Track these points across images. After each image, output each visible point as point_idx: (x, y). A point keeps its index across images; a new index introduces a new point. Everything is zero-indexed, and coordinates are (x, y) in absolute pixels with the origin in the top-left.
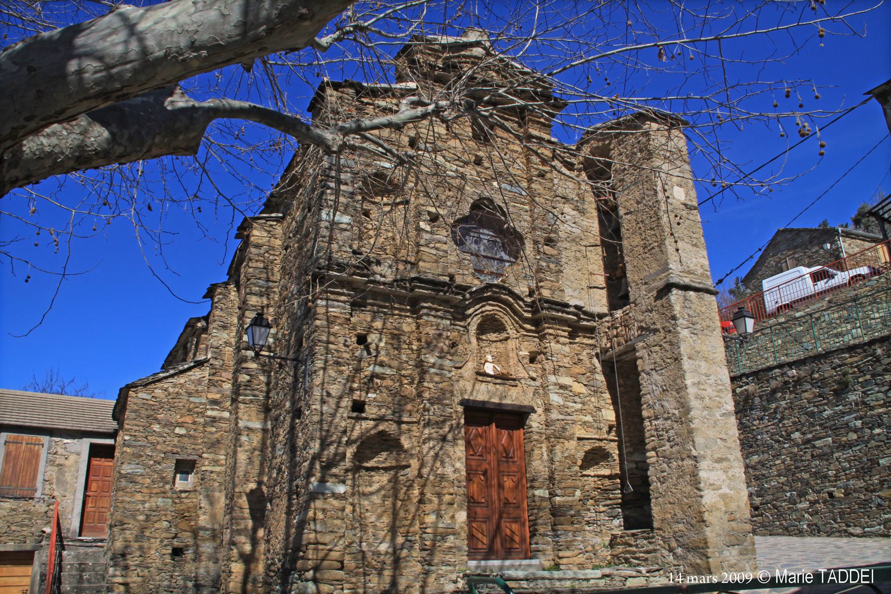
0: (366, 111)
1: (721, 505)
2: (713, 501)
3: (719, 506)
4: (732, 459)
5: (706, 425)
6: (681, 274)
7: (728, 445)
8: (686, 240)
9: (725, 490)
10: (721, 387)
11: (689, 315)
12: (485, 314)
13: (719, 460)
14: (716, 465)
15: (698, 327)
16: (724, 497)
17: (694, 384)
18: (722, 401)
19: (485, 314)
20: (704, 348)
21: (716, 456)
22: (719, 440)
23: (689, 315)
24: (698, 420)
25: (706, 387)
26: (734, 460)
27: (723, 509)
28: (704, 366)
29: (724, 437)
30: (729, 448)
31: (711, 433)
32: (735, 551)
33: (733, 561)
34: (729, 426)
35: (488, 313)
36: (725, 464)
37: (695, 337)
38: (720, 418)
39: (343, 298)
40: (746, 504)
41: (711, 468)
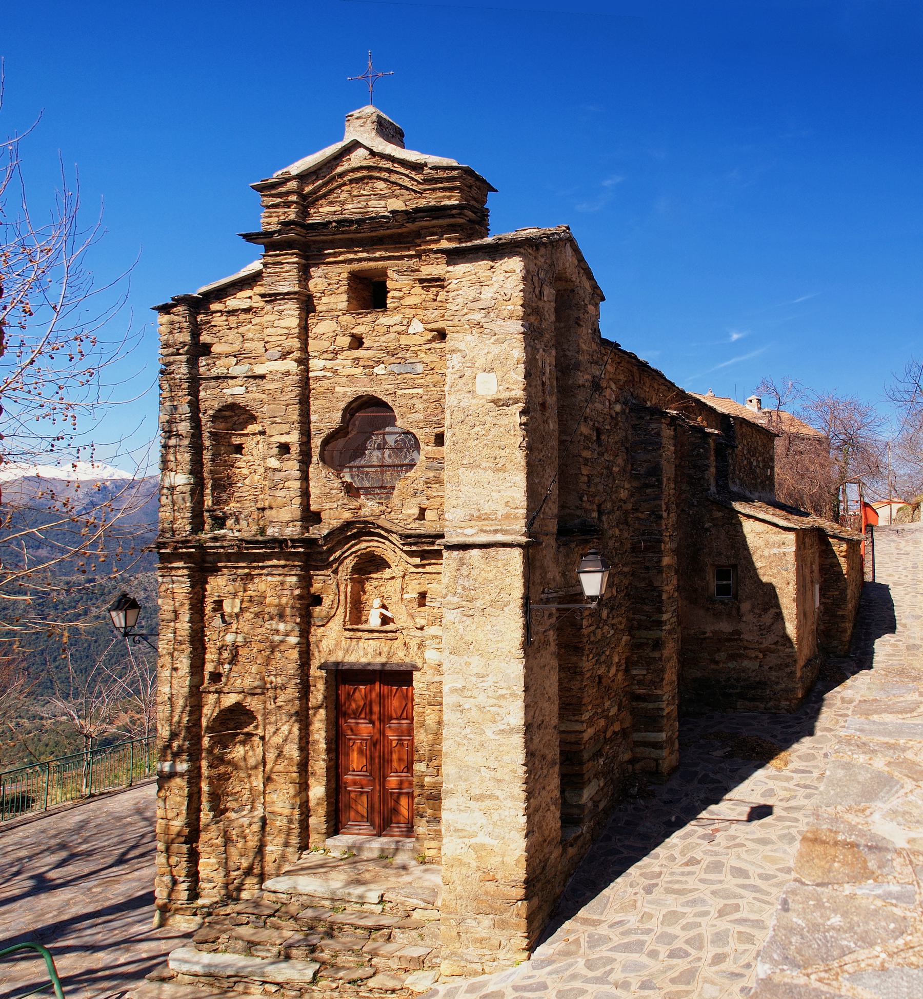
0: (213, 323)
1: (471, 858)
2: (458, 852)
3: (466, 860)
4: (501, 797)
5: (465, 748)
6: (463, 524)
7: (499, 775)
8: (484, 465)
9: (482, 839)
10: (504, 692)
11: (464, 588)
12: (359, 553)
13: (480, 798)
14: (472, 803)
15: (479, 604)
16: (478, 849)
17: (454, 690)
18: (502, 711)
19: (359, 553)
20: (481, 636)
21: (476, 791)
22: (483, 769)
23: (464, 588)
24: (451, 742)
25: (475, 693)
26: (505, 799)
27: (474, 864)
28: (477, 665)
29: (492, 765)
30: (499, 781)
31: (476, 759)
32: (486, 921)
33: (799, 937)
34: (505, 748)
35: (363, 551)
36: (488, 803)
37: (469, 621)
38: (493, 737)
39: (180, 572)
40: (518, 861)
41: (462, 808)
